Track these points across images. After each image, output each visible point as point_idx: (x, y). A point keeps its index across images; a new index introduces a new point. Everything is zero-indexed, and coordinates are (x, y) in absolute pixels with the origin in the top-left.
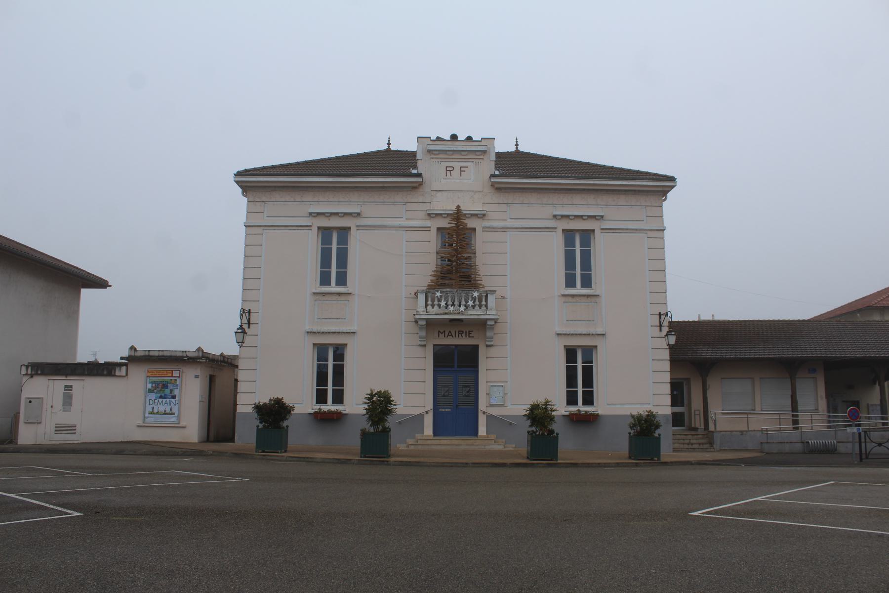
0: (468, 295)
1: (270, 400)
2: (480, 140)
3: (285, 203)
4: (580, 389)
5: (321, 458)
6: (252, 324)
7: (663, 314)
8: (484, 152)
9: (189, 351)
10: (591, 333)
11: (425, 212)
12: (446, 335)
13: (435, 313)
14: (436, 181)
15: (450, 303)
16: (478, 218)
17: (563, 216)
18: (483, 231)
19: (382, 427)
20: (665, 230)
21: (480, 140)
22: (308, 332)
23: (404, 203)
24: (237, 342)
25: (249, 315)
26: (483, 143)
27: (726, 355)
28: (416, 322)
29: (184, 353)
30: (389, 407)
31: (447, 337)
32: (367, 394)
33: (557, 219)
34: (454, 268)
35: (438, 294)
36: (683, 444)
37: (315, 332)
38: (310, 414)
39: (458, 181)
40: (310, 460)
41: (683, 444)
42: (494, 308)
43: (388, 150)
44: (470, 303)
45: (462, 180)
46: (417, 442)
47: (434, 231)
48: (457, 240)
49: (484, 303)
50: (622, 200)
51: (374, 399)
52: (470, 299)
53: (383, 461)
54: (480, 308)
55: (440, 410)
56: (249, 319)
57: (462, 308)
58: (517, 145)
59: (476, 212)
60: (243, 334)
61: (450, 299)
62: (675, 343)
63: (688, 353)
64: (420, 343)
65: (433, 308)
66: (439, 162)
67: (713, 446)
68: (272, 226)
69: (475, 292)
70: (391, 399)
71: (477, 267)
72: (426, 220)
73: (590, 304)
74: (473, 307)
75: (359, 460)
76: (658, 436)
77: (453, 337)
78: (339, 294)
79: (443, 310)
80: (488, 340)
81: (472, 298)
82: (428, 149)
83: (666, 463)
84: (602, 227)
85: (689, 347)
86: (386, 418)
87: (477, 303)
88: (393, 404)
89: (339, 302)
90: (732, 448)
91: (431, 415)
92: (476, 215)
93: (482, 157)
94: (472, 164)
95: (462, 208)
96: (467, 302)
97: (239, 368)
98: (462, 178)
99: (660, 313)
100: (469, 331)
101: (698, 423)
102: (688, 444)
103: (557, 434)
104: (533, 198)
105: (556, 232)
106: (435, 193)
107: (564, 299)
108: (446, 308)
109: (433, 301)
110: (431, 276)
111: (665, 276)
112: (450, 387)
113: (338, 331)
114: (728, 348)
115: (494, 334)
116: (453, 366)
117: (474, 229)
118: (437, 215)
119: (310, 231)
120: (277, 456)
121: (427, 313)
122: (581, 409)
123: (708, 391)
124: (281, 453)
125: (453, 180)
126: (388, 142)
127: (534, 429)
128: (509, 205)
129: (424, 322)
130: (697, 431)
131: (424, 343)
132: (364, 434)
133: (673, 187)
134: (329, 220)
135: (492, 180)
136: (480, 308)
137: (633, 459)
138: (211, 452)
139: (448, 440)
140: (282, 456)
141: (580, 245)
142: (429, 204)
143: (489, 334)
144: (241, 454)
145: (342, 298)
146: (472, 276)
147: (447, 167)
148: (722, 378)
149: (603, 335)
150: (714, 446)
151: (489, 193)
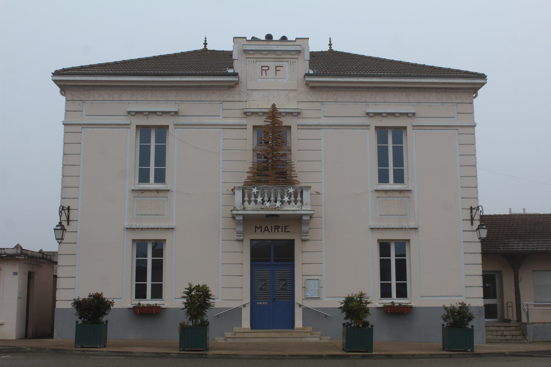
0: (284, 192)
1: (90, 296)
3: (103, 102)
4: (394, 282)
5: (140, 352)
6: (72, 221)
7: (474, 209)
8: (299, 52)
9: (7, 248)
10: (404, 227)
11: (242, 110)
12: (263, 230)
13: (252, 209)
14: (251, 81)
15: (266, 198)
17: (376, 114)
18: (298, 129)
19: (201, 320)
20: (475, 126)
22: (127, 228)
23: (221, 102)
24: (56, 239)
25: (69, 212)
26: (298, 42)
27: (537, 248)
28: (234, 217)
29: (2, 250)
30: (207, 301)
31: (264, 232)
32: (186, 289)
33: (370, 116)
35: (255, 190)
36: (496, 335)
37: (134, 229)
38: (129, 309)
39: (273, 80)
40: (129, 354)
41: (496, 335)
42: (309, 203)
43: (205, 50)
44: (286, 199)
45: (276, 79)
46: (235, 335)
47: (250, 129)
48: (273, 137)
49: (299, 198)
50: (433, 97)
51: (193, 293)
52: (286, 195)
53: (202, 354)
54: (296, 204)
55: (257, 303)
56: (69, 216)
57: (278, 204)
58: (330, 45)
59: (291, 111)
60: (62, 231)
61: (266, 195)
62: (487, 237)
63: (499, 246)
64: (237, 238)
65: (249, 204)
67: (525, 338)
68: (91, 124)
69: (290, 188)
70: (209, 293)
71: (292, 164)
73: (403, 199)
74: (289, 202)
75: (178, 353)
76: (471, 328)
77: (269, 232)
78: (158, 191)
79: (259, 206)
80: (303, 234)
81: (288, 194)
82: (244, 49)
83: (479, 355)
84: (414, 124)
85: (500, 240)
86: (204, 312)
87: (293, 198)
88: (211, 298)
89: (158, 198)
90: (545, 340)
91: (248, 308)
92: (291, 113)
95: (277, 106)
96: (282, 197)
97: (59, 264)
98: (276, 77)
99: (471, 207)
100: (285, 226)
101: (511, 314)
102: (501, 336)
103: (372, 326)
104: (346, 96)
105: (369, 129)
106: (251, 92)
107: (377, 194)
108: (263, 204)
109: (250, 197)
110: (248, 172)
111: (476, 171)
112: (267, 280)
113: (157, 227)
114: (540, 241)
115: (309, 229)
116: (270, 261)
117: (289, 127)
118: (253, 113)
119: (128, 129)
120: (97, 351)
121: (244, 209)
122: (395, 301)
123: (520, 283)
124: (100, 348)
125: (268, 80)
127: (349, 321)
128: (322, 103)
129: (241, 218)
130: (510, 322)
131: (241, 238)
132: (183, 328)
133: (483, 84)
134: (147, 118)
136: (296, 204)
137: (447, 351)
138: (30, 349)
139: (266, 333)
140: (102, 351)
143: (304, 229)
144: (60, 350)
145: (161, 194)
146: (288, 172)
147: (262, 67)
148: (534, 271)
149: (416, 229)
150: (528, 338)
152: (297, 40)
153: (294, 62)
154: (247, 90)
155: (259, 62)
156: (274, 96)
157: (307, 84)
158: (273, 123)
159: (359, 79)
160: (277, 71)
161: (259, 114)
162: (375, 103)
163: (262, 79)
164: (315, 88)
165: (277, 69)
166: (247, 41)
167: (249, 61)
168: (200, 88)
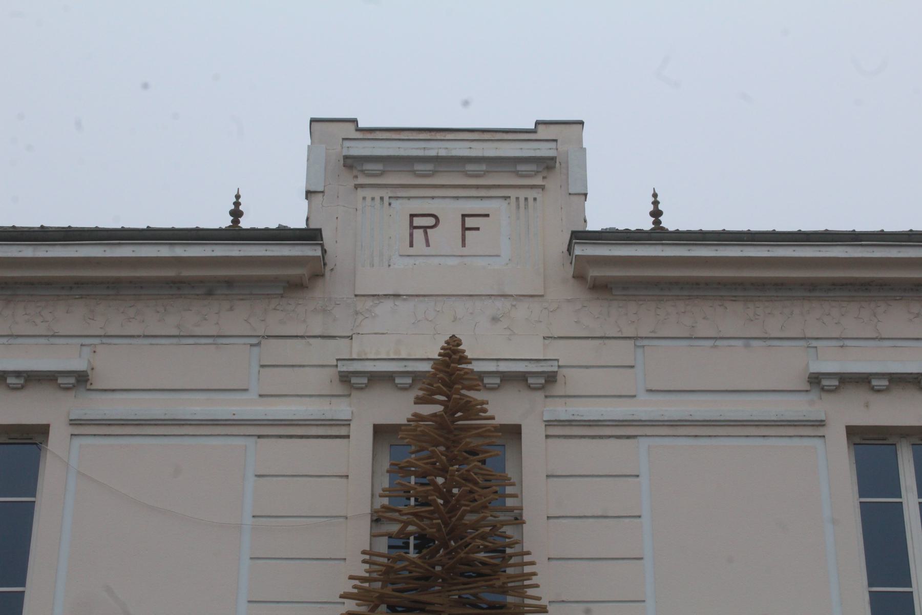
2: (533, 127)
8: (547, 164)
11: (334, 369)
16: (530, 388)
18: (547, 437)
21: (533, 127)
23: (254, 341)
26: (543, 133)
33: (823, 389)
34: (438, 568)
45: (466, 260)
47: (362, 437)
66: (386, 200)
71: (527, 559)
72: (334, 400)
82: (345, 153)
93: (538, 181)
94: (503, 204)
95: (469, 349)
98: (465, 251)
106: (369, 303)
117: (514, 432)
118: (376, 379)
125: (436, 261)
126: (233, 207)
128: (639, 343)
135: (578, 251)
141: (918, 495)
142: (347, 340)
151: (568, 301)
152: (540, 127)
153: (531, 201)
154: (356, 296)
155: (400, 201)
156: (455, 319)
157: (579, 277)
158: (451, 409)
159: (775, 249)
160: (467, 233)
161: (398, 381)
162: (841, 343)
163: (411, 261)
164: (611, 289)
165: (467, 226)
166: (358, 130)
167: (364, 198)
168: (179, 288)
